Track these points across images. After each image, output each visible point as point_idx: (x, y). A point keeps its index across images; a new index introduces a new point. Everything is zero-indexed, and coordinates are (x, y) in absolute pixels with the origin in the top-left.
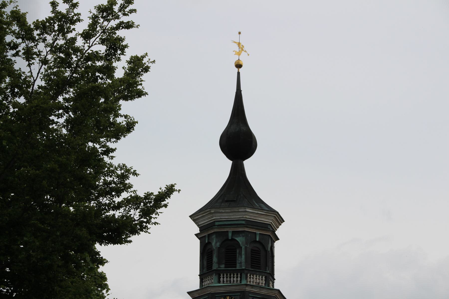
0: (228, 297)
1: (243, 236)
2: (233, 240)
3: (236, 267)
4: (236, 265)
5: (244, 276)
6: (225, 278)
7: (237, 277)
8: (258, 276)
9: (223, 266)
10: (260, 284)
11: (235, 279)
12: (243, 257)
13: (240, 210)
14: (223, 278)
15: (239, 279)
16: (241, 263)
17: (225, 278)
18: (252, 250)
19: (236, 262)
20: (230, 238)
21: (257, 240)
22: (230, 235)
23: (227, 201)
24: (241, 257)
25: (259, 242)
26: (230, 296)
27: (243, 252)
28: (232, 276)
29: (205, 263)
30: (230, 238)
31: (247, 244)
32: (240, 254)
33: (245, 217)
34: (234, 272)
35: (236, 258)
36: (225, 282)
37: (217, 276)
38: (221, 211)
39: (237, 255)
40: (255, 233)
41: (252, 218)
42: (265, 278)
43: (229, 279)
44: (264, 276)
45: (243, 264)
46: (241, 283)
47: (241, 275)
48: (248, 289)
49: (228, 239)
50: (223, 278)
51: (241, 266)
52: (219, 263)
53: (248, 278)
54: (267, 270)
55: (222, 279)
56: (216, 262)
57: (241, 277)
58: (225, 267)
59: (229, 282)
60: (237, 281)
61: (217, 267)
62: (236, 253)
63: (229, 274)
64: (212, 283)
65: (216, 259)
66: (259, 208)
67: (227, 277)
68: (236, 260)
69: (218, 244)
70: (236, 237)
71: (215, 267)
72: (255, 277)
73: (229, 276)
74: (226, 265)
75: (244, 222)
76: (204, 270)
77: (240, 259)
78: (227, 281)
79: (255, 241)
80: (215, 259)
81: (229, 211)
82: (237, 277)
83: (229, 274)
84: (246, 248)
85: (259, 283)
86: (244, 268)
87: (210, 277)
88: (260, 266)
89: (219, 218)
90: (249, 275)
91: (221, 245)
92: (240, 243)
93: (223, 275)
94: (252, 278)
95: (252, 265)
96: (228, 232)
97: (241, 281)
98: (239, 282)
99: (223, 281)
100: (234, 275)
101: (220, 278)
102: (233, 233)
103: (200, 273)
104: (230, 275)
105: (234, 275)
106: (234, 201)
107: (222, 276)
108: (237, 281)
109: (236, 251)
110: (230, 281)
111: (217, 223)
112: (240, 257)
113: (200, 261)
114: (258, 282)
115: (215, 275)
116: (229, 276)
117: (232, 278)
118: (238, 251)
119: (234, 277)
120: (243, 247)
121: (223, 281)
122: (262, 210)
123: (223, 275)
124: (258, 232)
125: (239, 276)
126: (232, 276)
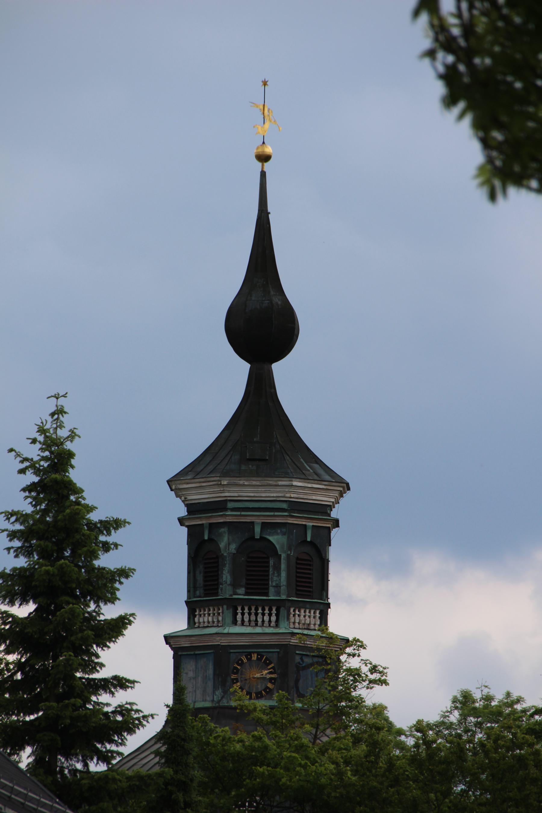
0: (256, 655)
1: (284, 534)
2: (262, 539)
3: (267, 594)
4: (268, 589)
5: (283, 611)
6: (246, 616)
7: (270, 615)
8: (308, 611)
9: (242, 590)
10: (312, 627)
11: (266, 618)
12: (283, 574)
13: (280, 483)
14: (243, 614)
15: (274, 618)
16: (278, 586)
17: (246, 616)
18: (298, 559)
19: (268, 584)
20: (257, 536)
21: (309, 539)
22: (257, 529)
23: (250, 460)
24: (279, 575)
25: (311, 542)
26: (258, 654)
27: (283, 566)
28: (260, 611)
29: (200, 579)
30: (257, 536)
31: (290, 549)
32: (277, 568)
33: (288, 495)
34: (263, 604)
35: (268, 575)
36: (246, 623)
37: (231, 610)
38: (241, 482)
39: (271, 570)
40: (305, 526)
41: (301, 496)
42: (319, 614)
43: (253, 618)
44: (318, 609)
45: (283, 589)
46: (277, 626)
47: (278, 610)
48: (294, 641)
49: (252, 538)
50: (243, 614)
51: (278, 593)
52: (235, 585)
53: (292, 615)
54: (325, 597)
55: (239, 617)
56: (229, 582)
57: (277, 615)
58: (247, 594)
59: (253, 623)
60: (270, 621)
61: (231, 592)
62: (268, 567)
63: (253, 608)
64: (218, 621)
65: (229, 577)
66: (316, 477)
67: (250, 614)
68: (268, 580)
69: (233, 548)
70: (269, 535)
71: (226, 592)
72: (304, 614)
73: (253, 611)
74: (247, 588)
75: (285, 506)
76: (198, 593)
77: (275, 578)
78: (250, 621)
79: (305, 541)
80: (226, 576)
81: (258, 483)
82: (270, 615)
83: (253, 608)
84: (288, 556)
85: (309, 624)
86: (284, 597)
87: (214, 610)
88: (311, 590)
89: (236, 494)
90: (292, 610)
91: (238, 549)
92: (277, 547)
93: (243, 609)
94: (297, 615)
95: (297, 590)
96: (253, 523)
97: (277, 621)
98: (273, 624)
99: (243, 621)
100: (263, 610)
101: (237, 614)
102: (264, 525)
103: (189, 597)
104: (257, 609)
105: (263, 610)
106: (265, 460)
107: (239, 611)
108: (270, 621)
109: (268, 562)
110: (256, 621)
111: (230, 505)
112: (276, 575)
113: (189, 572)
114: (309, 623)
115: (227, 609)
116: (253, 611)
117: (260, 616)
118: (271, 562)
119: (263, 614)
120: (283, 556)
121: (243, 621)
122: (321, 480)
123: (243, 609)
124: (310, 524)
125: (274, 611)
126: (260, 611)
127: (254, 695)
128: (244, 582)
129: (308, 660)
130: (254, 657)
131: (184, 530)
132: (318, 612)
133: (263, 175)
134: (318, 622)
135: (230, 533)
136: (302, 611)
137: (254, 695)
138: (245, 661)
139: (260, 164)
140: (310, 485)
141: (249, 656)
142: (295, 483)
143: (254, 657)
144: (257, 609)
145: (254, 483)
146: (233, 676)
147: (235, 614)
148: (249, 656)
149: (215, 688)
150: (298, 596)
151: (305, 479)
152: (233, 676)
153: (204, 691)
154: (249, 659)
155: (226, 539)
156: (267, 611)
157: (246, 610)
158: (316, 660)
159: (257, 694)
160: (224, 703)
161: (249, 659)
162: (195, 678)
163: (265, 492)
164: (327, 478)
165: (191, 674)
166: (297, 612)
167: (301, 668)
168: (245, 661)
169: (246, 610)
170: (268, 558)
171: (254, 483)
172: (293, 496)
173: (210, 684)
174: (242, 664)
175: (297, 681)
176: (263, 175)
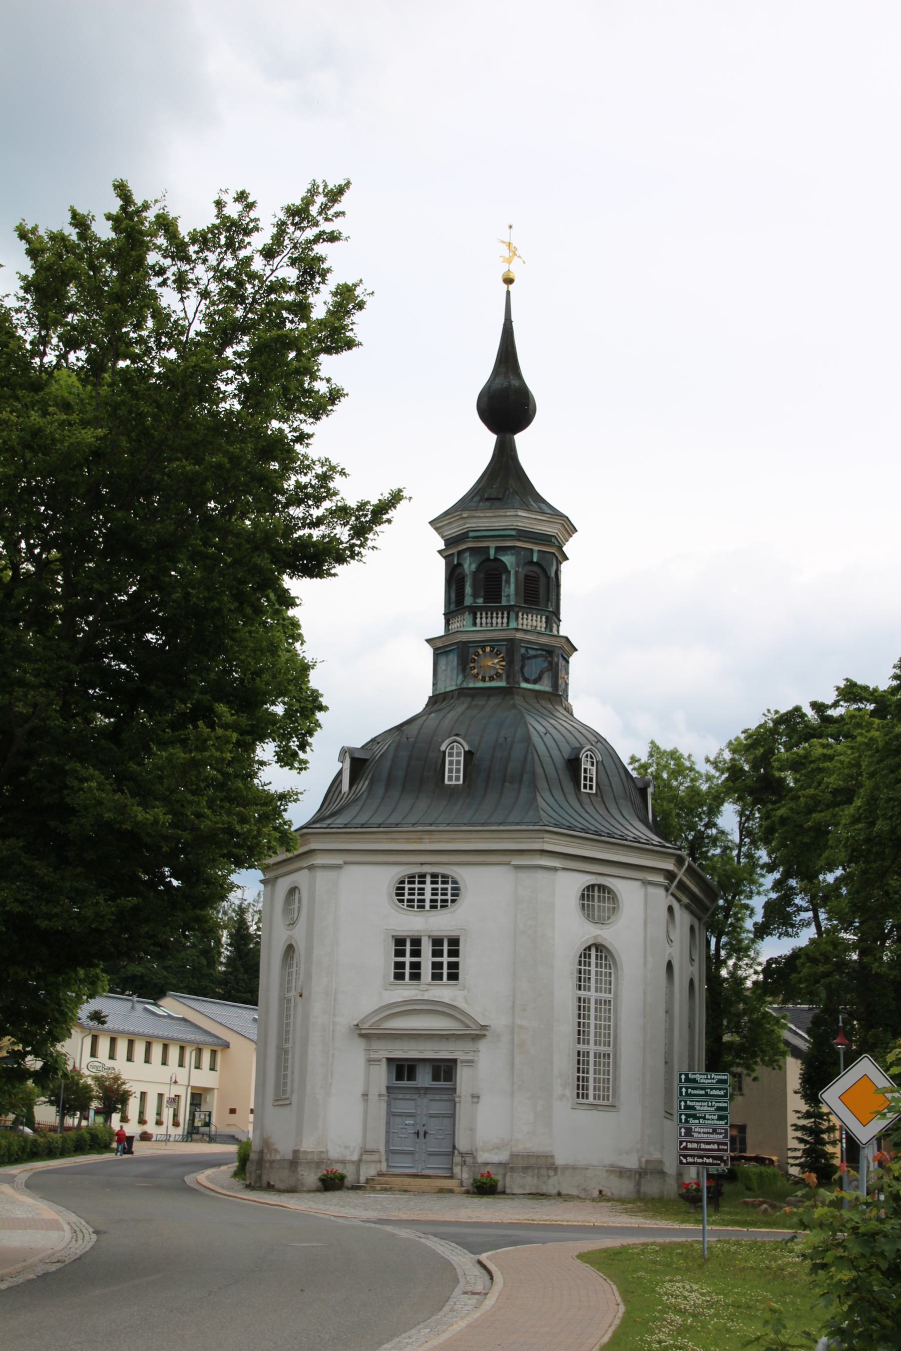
1: (513, 555)
2: (496, 559)
3: (500, 602)
4: (501, 598)
5: (512, 615)
7: (502, 618)
12: (512, 586)
13: (508, 514)
14: (481, 618)
15: (505, 620)
16: (508, 596)
17: (484, 620)
18: (526, 576)
19: (501, 595)
20: (492, 557)
21: (535, 560)
22: (492, 552)
24: (509, 587)
27: (512, 580)
30: (492, 557)
31: (518, 566)
32: (508, 582)
34: (497, 609)
35: (501, 588)
38: (478, 515)
40: (532, 550)
45: (512, 597)
47: (508, 614)
51: (509, 601)
52: (475, 596)
55: (478, 621)
57: (508, 618)
69: (473, 567)
70: (502, 555)
71: (468, 601)
75: (513, 533)
80: (468, 590)
81: (491, 515)
82: (502, 618)
86: (513, 603)
90: (520, 614)
91: (478, 568)
93: (481, 614)
96: (488, 547)
102: (498, 549)
107: (478, 615)
111: (471, 534)
118: (504, 578)
120: (512, 572)
122: (543, 513)
123: (481, 614)
124: (536, 548)
125: (505, 615)
126: (495, 615)
127: (487, 679)
128: (482, 594)
129: (532, 653)
130: (488, 649)
131: (442, 562)
132: (544, 618)
133: (508, 293)
134: (544, 625)
135: (471, 555)
136: (530, 616)
137: (487, 679)
138: (481, 652)
139: (506, 286)
140: (534, 516)
141: (483, 648)
142: (520, 514)
143: (488, 649)
144: (492, 614)
145: (488, 515)
146: (472, 665)
147: (475, 618)
148: (483, 648)
149: (458, 675)
150: (525, 603)
151: (530, 511)
152: (472, 665)
153: (452, 678)
154: (484, 651)
155: (468, 562)
156: (500, 615)
157: (484, 615)
158: (540, 652)
159: (490, 677)
160: (465, 685)
161: (484, 651)
162: (446, 670)
163: (497, 522)
164: (550, 512)
165: (444, 667)
166: (525, 616)
167: (524, 658)
168: (481, 652)
169: (484, 615)
170: (501, 574)
171: (488, 515)
172: (521, 524)
173: (455, 672)
174: (478, 655)
175: (522, 667)
176: (508, 293)
